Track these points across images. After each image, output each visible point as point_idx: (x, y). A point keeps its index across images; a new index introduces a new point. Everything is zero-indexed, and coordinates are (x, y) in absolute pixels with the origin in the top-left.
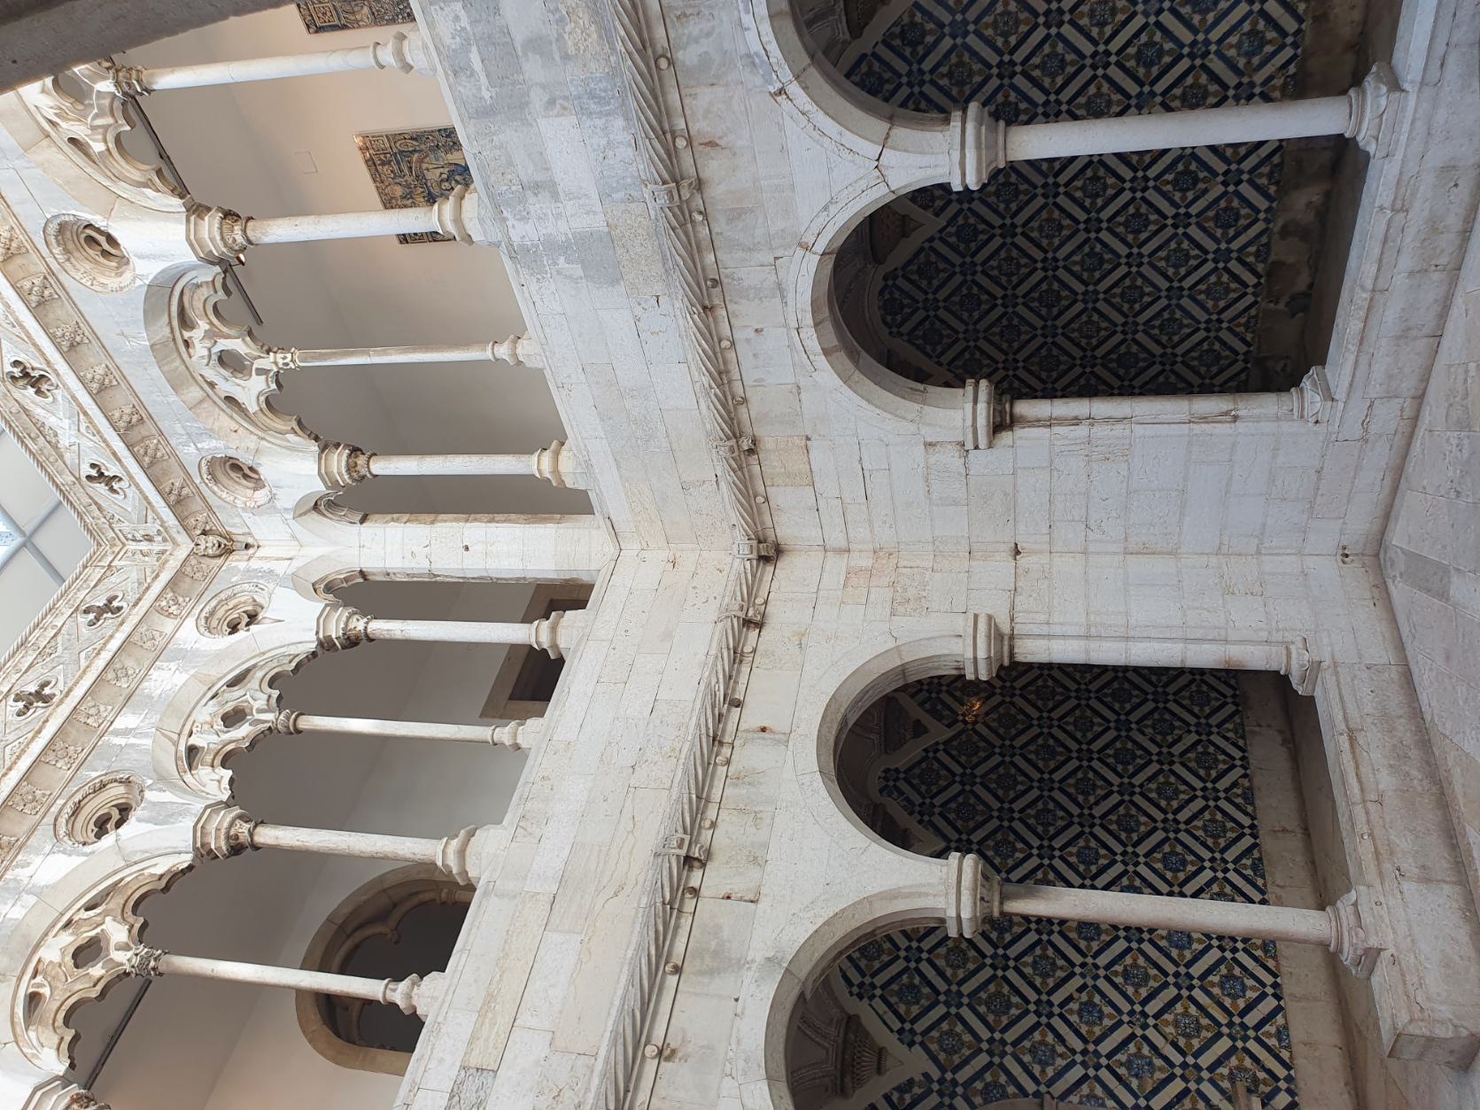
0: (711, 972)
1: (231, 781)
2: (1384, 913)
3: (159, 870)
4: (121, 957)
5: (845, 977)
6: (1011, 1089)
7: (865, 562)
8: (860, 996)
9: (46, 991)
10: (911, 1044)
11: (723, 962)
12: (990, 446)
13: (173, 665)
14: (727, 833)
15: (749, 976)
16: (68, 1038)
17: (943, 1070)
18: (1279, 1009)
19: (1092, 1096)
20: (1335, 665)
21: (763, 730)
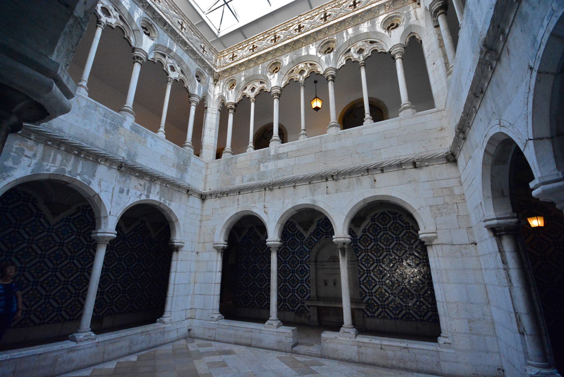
0: (311, 189)
1: (343, 65)
2: (348, 339)
3: (319, 70)
4: (301, 79)
5: (376, 215)
6: (358, 255)
7: (457, 191)
8: (372, 219)
10: (363, 232)
11: (313, 192)
12: (487, 227)
13: (369, 25)
14: (343, 182)
15: (311, 197)
17: (359, 240)
18: (392, 318)
19: (360, 272)
20: (437, 351)
21: (375, 181)
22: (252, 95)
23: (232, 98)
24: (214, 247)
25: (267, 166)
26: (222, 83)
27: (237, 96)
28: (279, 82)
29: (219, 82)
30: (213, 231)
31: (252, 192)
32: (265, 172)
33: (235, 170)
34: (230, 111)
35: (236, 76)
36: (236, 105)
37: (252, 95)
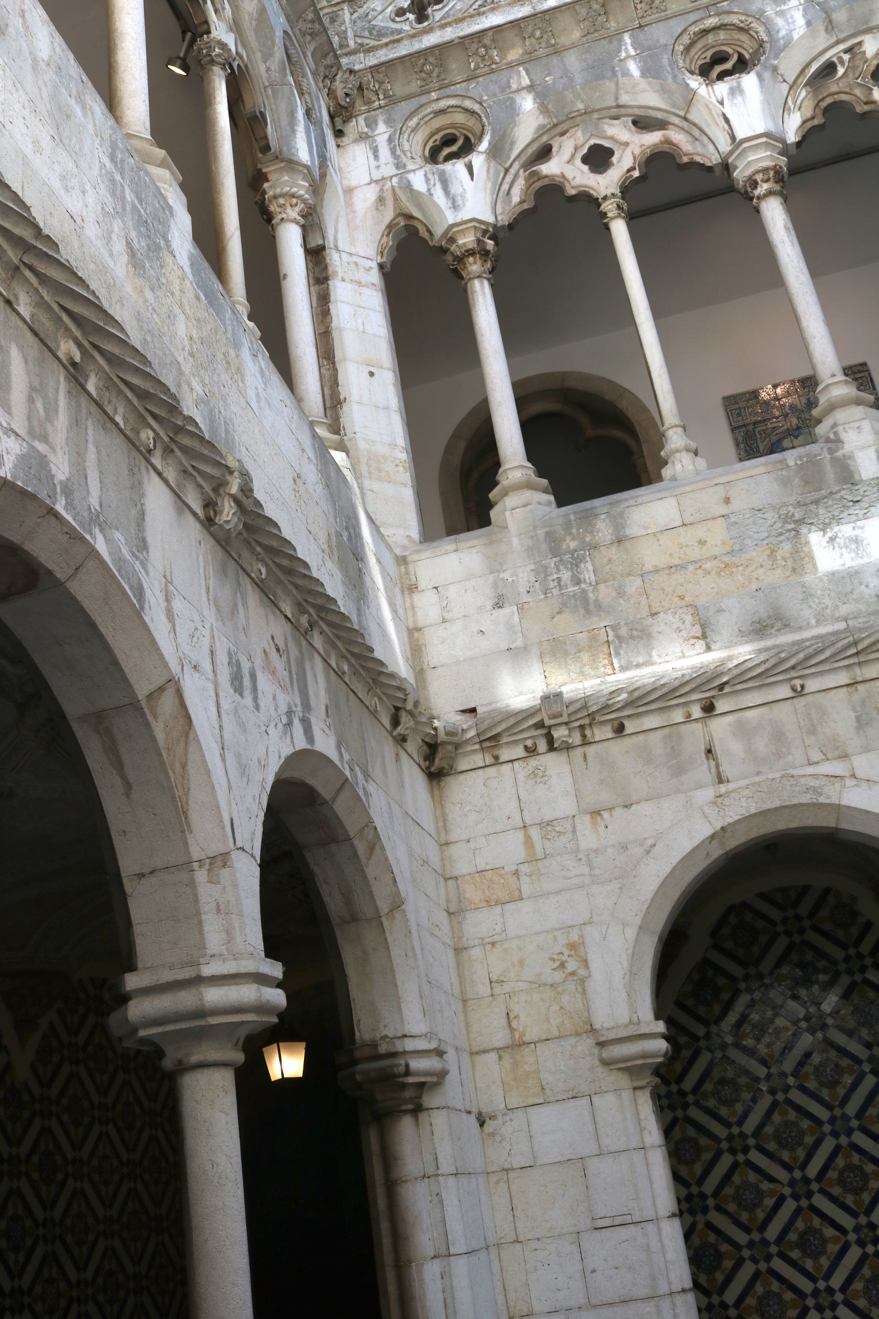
9: (841, 71)
16: (816, 122)
22: (605, 184)
23: (470, 198)
24: (606, 1063)
25: (856, 541)
26: (381, 127)
27: (499, 193)
28: (773, 118)
29: (359, 124)
30: (572, 961)
31: (799, 693)
32: (852, 575)
33: (633, 585)
34: (474, 266)
35: (480, 93)
36: (495, 233)
37: (605, 184)
